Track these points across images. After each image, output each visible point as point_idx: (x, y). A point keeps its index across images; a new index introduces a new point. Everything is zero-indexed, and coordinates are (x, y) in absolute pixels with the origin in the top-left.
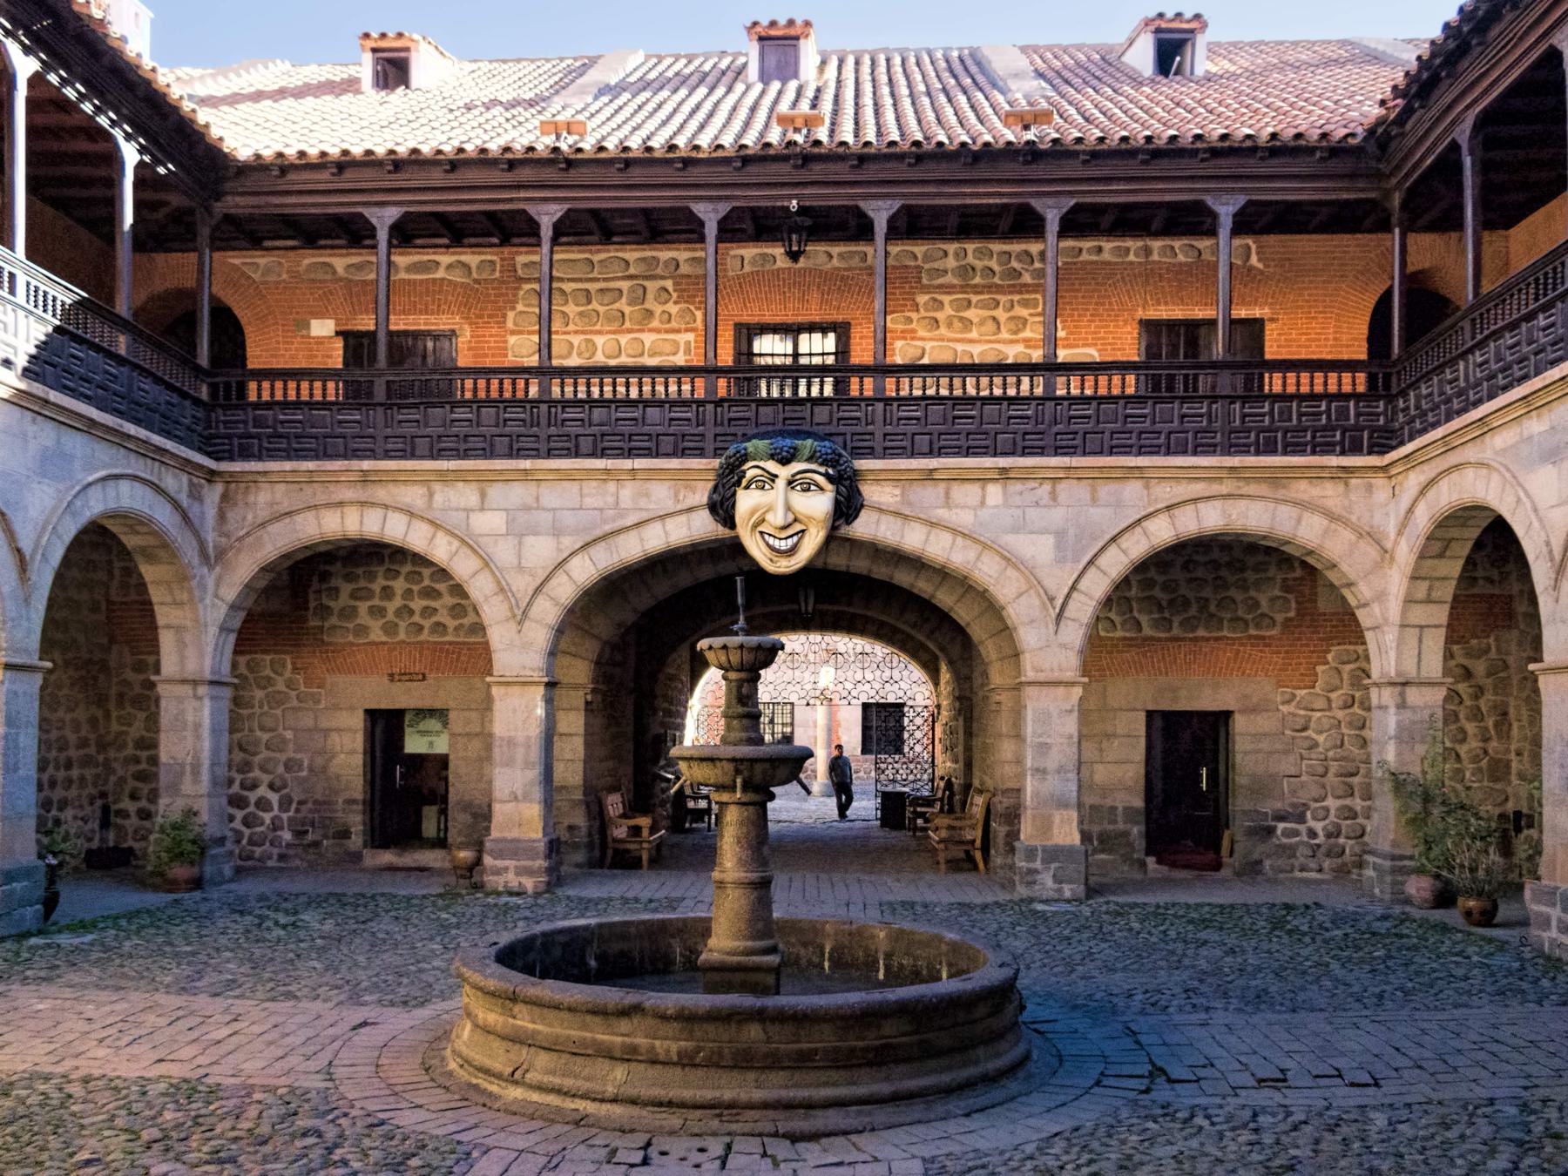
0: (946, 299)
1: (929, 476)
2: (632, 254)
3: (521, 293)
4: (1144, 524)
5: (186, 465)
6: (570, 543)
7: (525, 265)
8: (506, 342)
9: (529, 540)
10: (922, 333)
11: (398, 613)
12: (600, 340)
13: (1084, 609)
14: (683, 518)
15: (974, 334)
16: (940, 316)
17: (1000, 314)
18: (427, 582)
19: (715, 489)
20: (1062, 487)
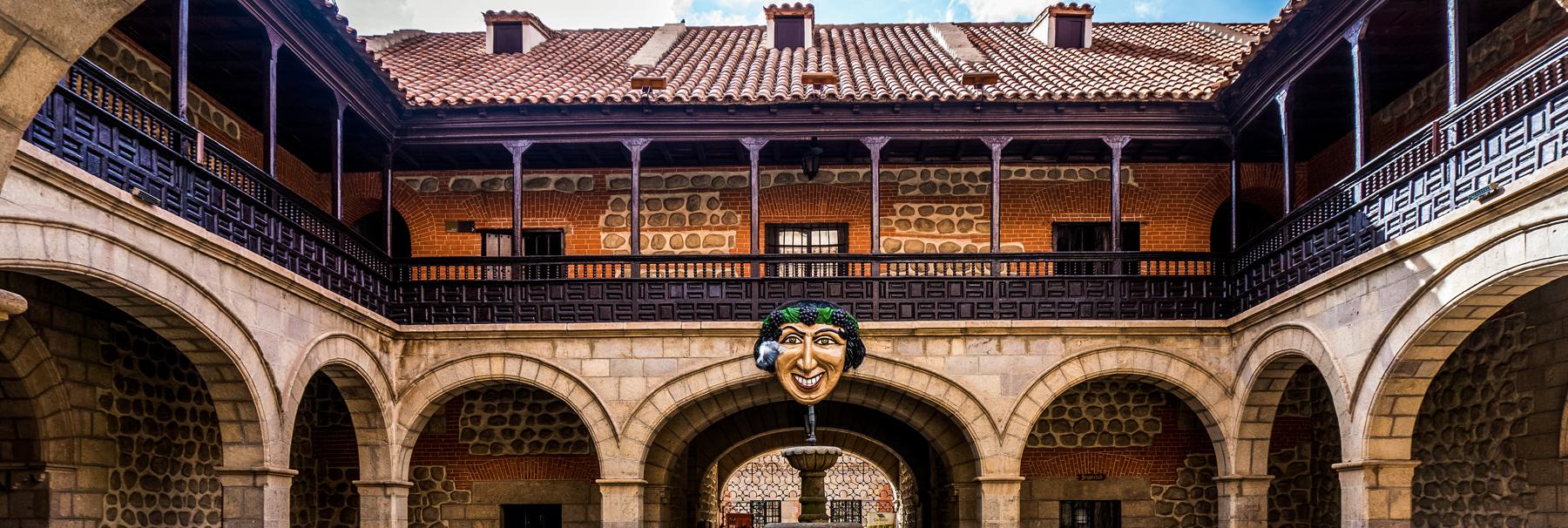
0: (916, 207)
1: (912, 334)
2: (690, 174)
3: (609, 202)
4: (1063, 368)
5: (379, 328)
6: (656, 382)
7: (611, 182)
8: (600, 237)
9: (626, 381)
10: (898, 231)
11: (523, 433)
12: (667, 236)
13: (1021, 430)
14: (736, 364)
15: (936, 232)
16: (912, 219)
17: (954, 217)
18: (544, 412)
20: (1003, 342)
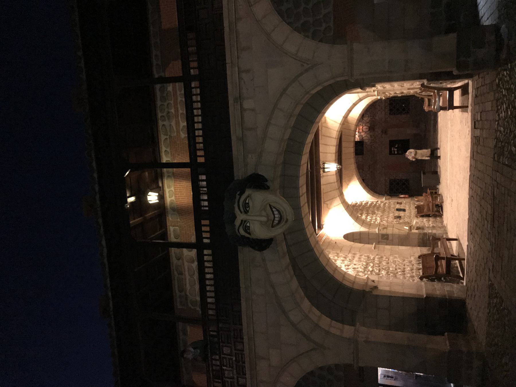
1: (242, 139)
3: (192, 307)
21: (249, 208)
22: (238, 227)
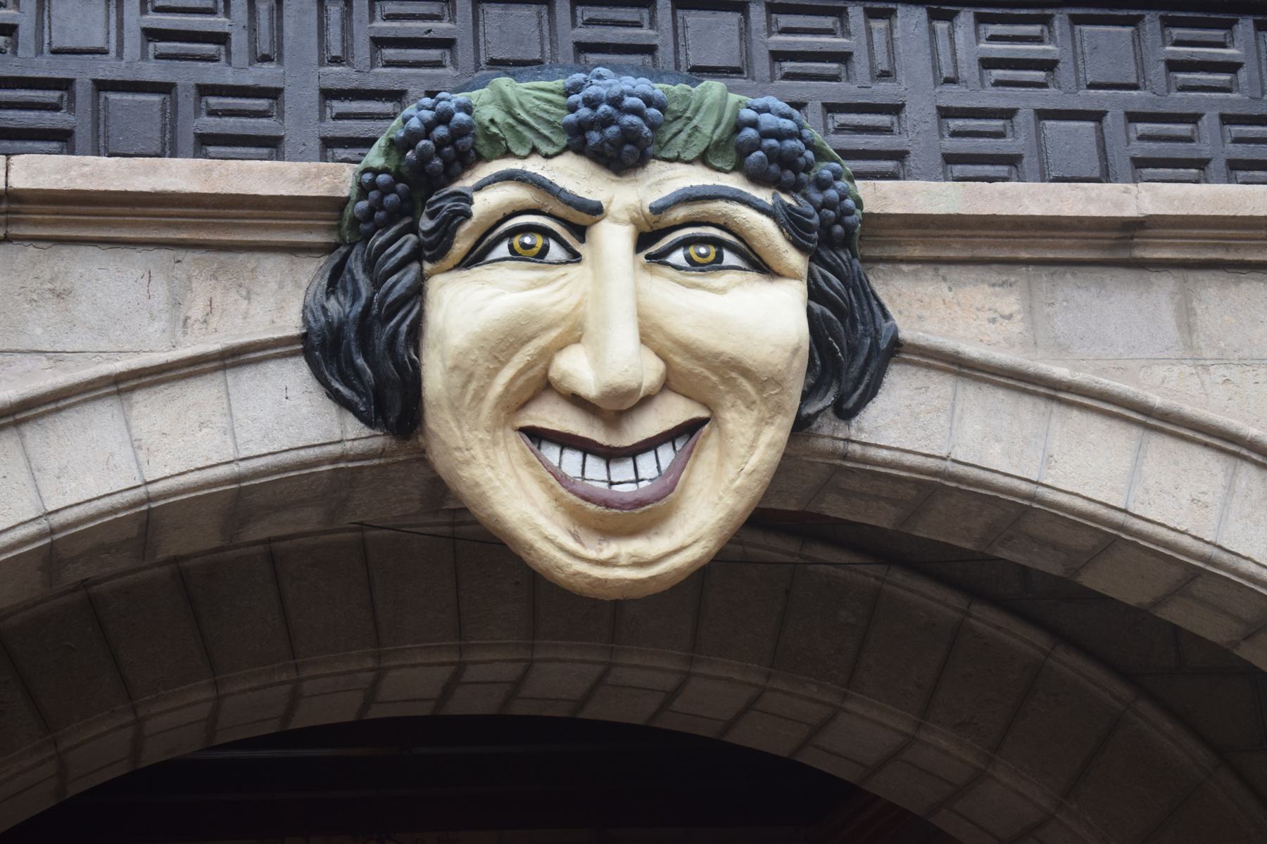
19: (336, 279)
21: (684, 263)
22: (548, 176)
